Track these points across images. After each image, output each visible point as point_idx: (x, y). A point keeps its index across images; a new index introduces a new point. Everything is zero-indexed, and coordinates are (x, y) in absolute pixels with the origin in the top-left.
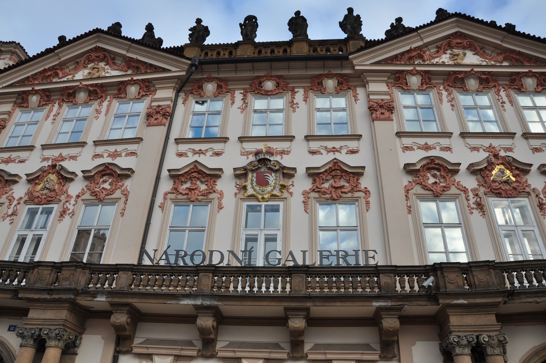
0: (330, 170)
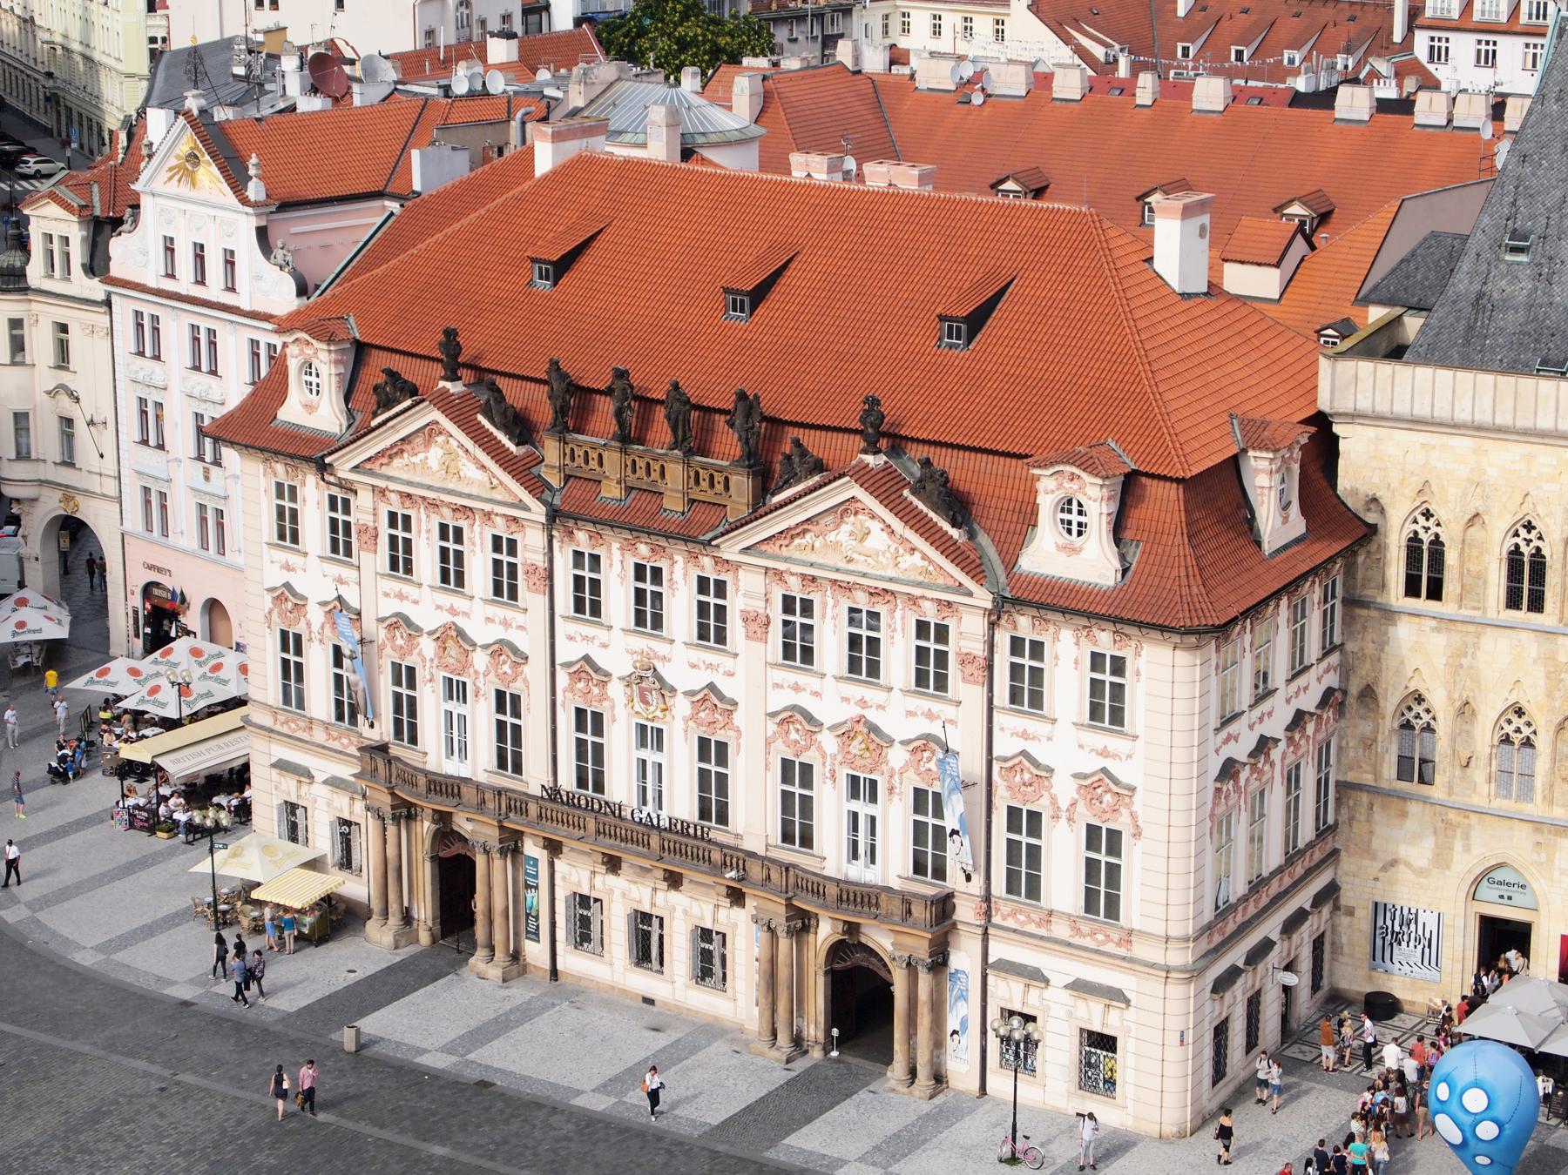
0: (704, 700)
